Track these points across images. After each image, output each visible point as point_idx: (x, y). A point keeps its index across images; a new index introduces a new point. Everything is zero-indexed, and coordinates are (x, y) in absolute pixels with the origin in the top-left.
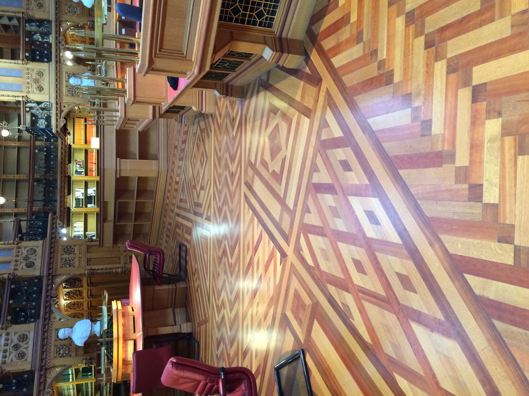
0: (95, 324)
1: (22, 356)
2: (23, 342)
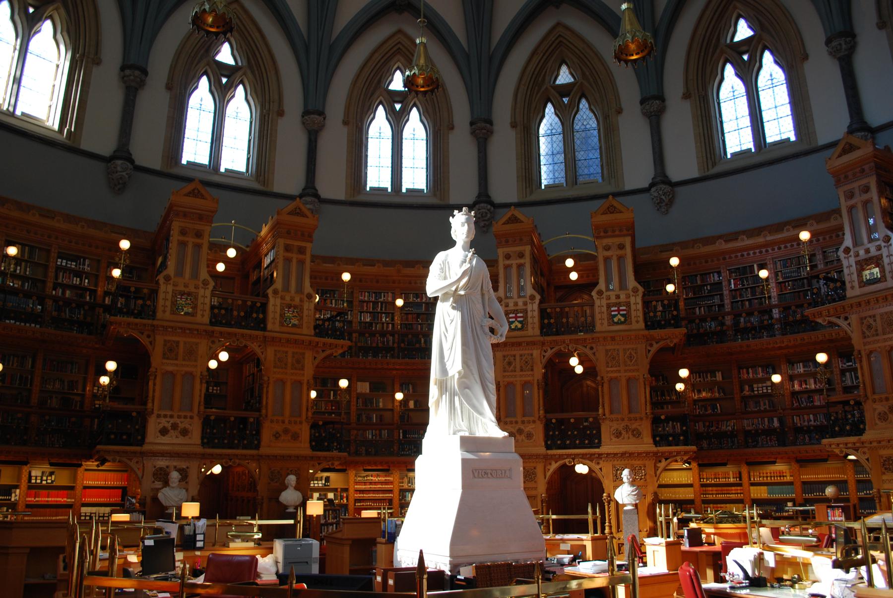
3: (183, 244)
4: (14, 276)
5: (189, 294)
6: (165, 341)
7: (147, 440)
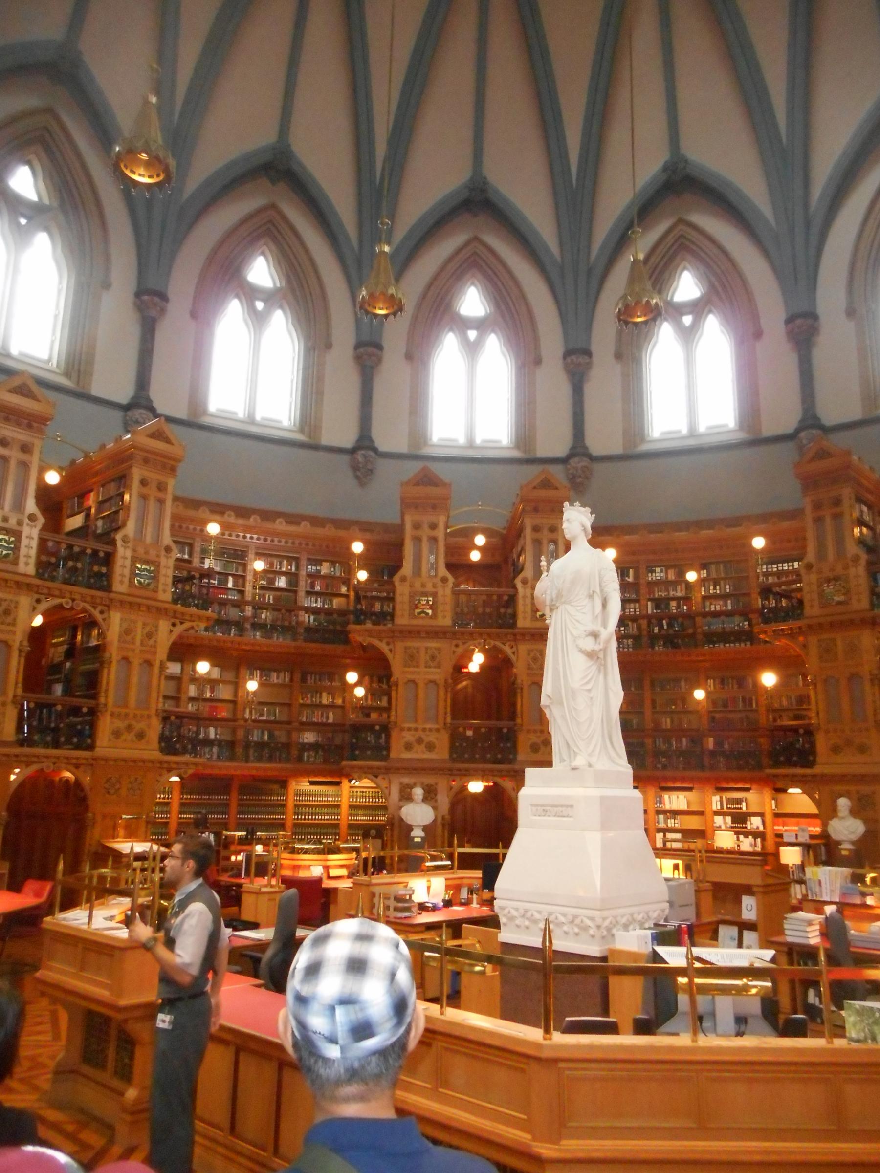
0: (423, 830)
1: (408, 747)
2: (426, 747)
3: (819, 520)
4: (715, 597)
5: (836, 579)
6: (819, 641)
7: (818, 760)
